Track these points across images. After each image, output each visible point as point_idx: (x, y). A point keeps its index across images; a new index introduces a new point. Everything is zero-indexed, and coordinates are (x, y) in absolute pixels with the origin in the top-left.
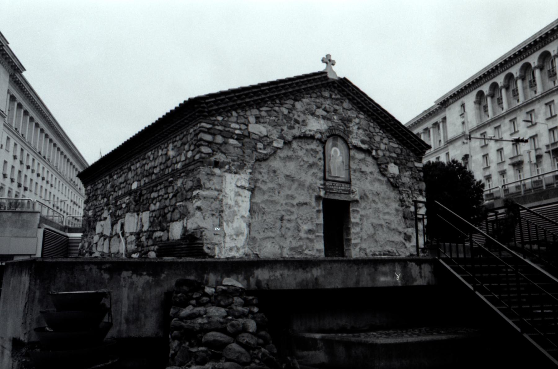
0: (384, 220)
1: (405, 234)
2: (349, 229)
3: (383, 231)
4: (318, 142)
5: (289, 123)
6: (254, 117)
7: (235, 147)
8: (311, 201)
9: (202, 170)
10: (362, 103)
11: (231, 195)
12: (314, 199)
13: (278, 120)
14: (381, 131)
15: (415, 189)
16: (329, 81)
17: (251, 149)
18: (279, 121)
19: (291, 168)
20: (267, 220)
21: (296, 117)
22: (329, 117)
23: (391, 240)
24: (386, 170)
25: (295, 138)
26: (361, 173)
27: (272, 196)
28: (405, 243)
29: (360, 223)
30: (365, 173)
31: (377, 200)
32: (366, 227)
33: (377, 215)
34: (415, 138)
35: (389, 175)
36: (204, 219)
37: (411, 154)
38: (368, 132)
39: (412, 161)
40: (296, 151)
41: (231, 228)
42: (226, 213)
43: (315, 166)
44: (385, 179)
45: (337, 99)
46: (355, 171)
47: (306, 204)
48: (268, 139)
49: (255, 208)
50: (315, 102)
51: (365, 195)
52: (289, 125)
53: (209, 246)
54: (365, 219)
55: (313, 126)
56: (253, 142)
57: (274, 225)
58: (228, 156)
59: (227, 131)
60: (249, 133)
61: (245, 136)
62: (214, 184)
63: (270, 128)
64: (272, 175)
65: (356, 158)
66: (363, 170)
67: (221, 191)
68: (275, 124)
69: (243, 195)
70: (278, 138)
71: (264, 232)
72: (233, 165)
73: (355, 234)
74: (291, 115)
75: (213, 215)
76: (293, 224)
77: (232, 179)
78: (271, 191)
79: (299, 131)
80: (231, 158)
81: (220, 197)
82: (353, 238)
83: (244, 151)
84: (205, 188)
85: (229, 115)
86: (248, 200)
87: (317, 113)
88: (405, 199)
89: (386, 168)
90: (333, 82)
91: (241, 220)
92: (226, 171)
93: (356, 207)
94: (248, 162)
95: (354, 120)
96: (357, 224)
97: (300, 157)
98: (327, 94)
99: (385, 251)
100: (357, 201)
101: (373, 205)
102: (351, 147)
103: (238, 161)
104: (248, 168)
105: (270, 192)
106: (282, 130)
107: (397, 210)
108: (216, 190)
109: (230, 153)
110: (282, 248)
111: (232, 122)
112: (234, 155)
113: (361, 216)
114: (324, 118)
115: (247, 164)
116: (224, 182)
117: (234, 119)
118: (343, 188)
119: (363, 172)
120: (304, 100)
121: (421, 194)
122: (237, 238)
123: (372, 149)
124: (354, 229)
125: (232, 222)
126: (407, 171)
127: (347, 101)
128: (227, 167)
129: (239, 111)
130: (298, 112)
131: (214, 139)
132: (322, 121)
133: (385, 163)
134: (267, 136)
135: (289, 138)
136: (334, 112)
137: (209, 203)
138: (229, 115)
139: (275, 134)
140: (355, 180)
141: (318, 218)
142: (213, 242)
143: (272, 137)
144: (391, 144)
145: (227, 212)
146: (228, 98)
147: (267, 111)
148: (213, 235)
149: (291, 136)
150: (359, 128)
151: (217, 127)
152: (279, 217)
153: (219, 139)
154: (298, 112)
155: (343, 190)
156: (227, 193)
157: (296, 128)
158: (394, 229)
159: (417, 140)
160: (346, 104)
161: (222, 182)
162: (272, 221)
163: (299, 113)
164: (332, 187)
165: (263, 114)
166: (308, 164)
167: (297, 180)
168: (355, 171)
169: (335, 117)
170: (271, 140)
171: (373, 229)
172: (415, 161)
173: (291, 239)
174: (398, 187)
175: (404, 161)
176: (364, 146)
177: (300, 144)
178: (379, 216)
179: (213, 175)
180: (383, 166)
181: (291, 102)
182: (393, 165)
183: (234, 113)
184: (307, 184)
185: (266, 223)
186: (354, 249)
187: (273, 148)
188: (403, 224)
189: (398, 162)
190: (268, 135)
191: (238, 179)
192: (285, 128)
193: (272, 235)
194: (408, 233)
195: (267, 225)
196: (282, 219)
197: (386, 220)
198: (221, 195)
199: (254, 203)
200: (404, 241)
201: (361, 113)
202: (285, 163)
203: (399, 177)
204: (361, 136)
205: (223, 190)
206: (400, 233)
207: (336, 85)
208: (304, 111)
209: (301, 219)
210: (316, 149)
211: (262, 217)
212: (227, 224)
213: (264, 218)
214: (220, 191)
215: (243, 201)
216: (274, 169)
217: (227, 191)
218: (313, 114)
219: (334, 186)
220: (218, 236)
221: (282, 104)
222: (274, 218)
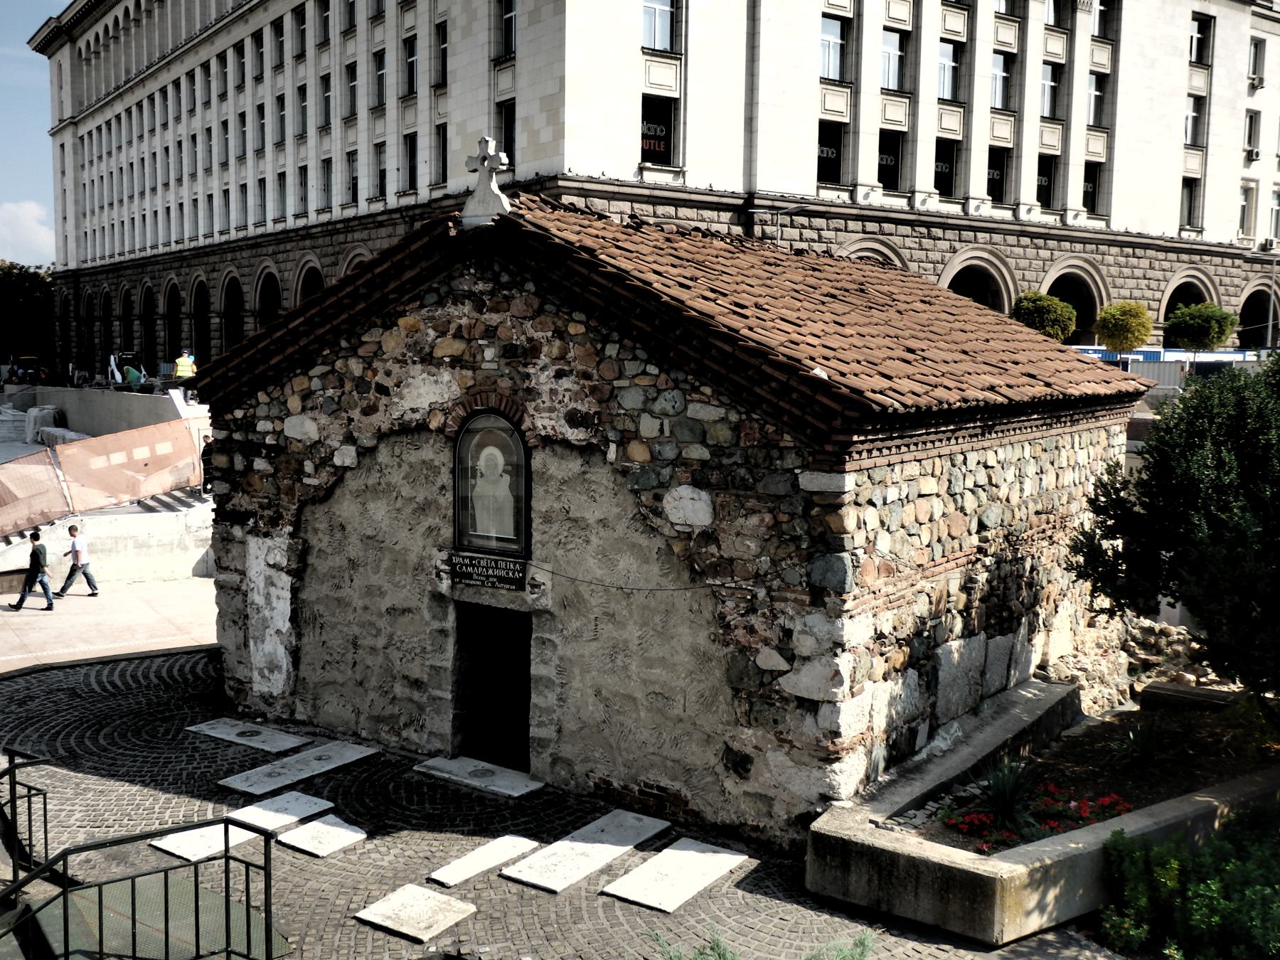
0: (645, 682)
5: (365, 398)
7: (263, 475)
11: (261, 583)
12: (426, 600)
13: (343, 393)
14: (652, 369)
15: (787, 586)
19: (379, 510)
20: (330, 644)
21: (379, 378)
24: (659, 513)
25: (381, 436)
26: (569, 524)
27: (339, 587)
29: (558, 682)
32: (579, 695)
33: (619, 662)
34: (783, 378)
37: (787, 440)
40: (386, 472)
42: (253, 622)
43: (433, 508)
44: (659, 542)
46: (547, 519)
47: (409, 610)
50: (432, 318)
51: (577, 594)
52: (365, 403)
53: (232, 683)
54: (577, 671)
55: (419, 395)
60: (287, 438)
63: (324, 419)
64: (338, 535)
65: (551, 477)
66: (571, 515)
68: (335, 407)
69: (280, 584)
70: (342, 443)
71: (323, 668)
72: (262, 517)
75: (234, 622)
86: (288, 595)
88: (733, 619)
91: (276, 638)
92: (249, 532)
95: (545, 349)
101: (607, 629)
102: (532, 442)
103: (269, 506)
106: (350, 420)
107: (703, 658)
108: (236, 570)
113: (561, 659)
114: (456, 362)
118: (503, 573)
119: (575, 520)
123: (607, 442)
124: (540, 693)
125: (263, 642)
128: (251, 522)
130: (385, 361)
131: (232, 462)
132: (446, 376)
133: (653, 488)
134: (319, 441)
135: (367, 442)
137: (229, 598)
138: (253, 402)
141: (441, 650)
143: (328, 442)
145: (253, 620)
146: (232, 369)
150: (559, 375)
155: (501, 579)
156: (253, 579)
157: (382, 408)
163: (389, 365)
164: (470, 569)
165: (316, 384)
167: (389, 549)
168: (547, 519)
169: (489, 353)
171: (601, 706)
172: (805, 467)
175: (742, 471)
176: (575, 435)
178: (625, 668)
182: (685, 491)
183: (262, 397)
184: (413, 558)
188: (723, 707)
189: (714, 477)
191: (269, 549)
192: (356, 414)
193: (340, 679)
194: (736, 746)
196: (355, 645)
197: (653, 683)
200: (720, 769)
203: (709, 536)
204: (566, 400)
208: (404, 355)
209: (398, 648)
210: (432, 460)
212: (255, 644)
213: (324, 638)
214: (243, 573)
215: (278, 598)
217: (252, 573)
218: (429, 360)
219: (473, 566)
221: (353, 351)
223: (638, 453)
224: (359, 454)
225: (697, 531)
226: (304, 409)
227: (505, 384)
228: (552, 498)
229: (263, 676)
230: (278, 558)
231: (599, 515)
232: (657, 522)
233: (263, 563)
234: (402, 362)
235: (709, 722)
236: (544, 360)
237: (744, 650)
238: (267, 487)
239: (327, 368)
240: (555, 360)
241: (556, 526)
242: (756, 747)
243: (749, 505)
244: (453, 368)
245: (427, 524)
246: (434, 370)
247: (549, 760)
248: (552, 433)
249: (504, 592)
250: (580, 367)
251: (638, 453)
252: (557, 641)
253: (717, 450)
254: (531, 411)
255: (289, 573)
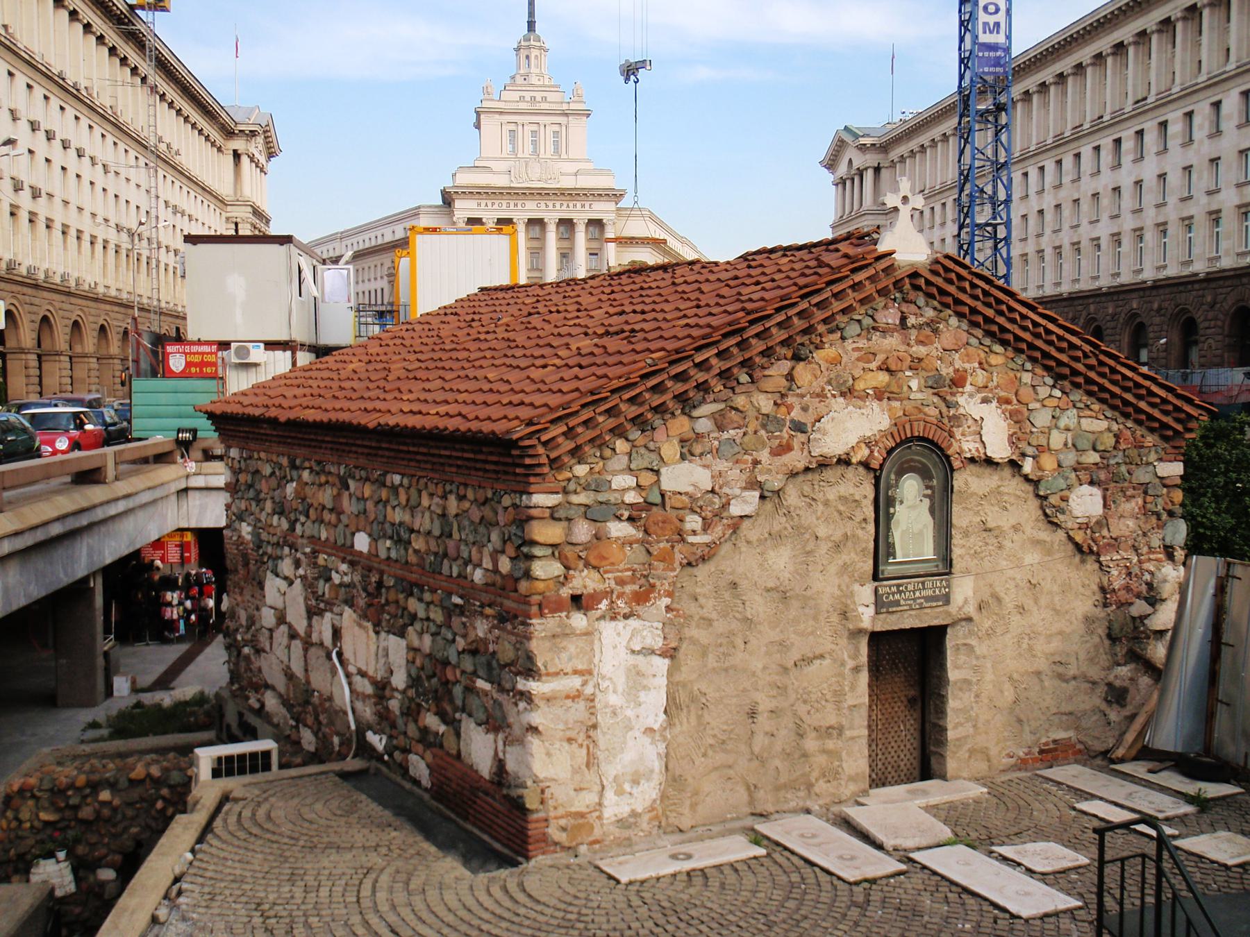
1: (1109, 685)
2: (942, 699)
3: (1043, 688)
4: (861, 469)
6: (676, 442)
8: (834, 647)
9: (537, 627)
10: (1001, 320)
12: (844, 642)
14: (1057, 393)
16: (899, 274)
17: (668, 541)
18: (746, 439)
19: (781, 560)
21: (796, 414)
22: (895, 389)
23: (1063, 710)
25: (793, 475)
26: (985, 534)
28: (1108, 711)
30: (996, 533)
31: (1028, 604)
32: (991, 687)
35: (1069, 525)
36: (548, 754)
37: (1150, 440)
38: (1015, 406)
39: (1148, 464)
41: (619, 767)
43: (849, 544)
44: (1061, 534)
45: (920, 327)
48: (717, 500)
49: (682, 697)
53: (563, 822)
56: (672, 514)
57: (732, 731)
58: (606, 572)
59: (601, 503)
61: (649, 505)
62: (570, 659)
63: (722, 465)
64: (727, 595)
65: (974, 494)
66: (991, 524)
67: (590, 672)
68: (737, 449)
70: (745, 489)
71: (704, 755)
72: (620, 596)
73: (956, 711)
74: (783, 409)
75: (570, 740)
76: (788, 721)
77: (619, 634)
78: (724, 641)
79: (805, 452)
80: (615, 578)
81: (589, 690)
82: (950, 726)
83: (651, 549)
84: (548, 674)
85: (608, 453)
86: (664, 681)
87: (860, 386)
89: (1063, 505)
90: (915, 275)
91: (646, 740)
92: (602, 617)
93: (965, 637)
94: (659, 578)
95: (969, 379)
96: (967, 682)
97: (807, 529)
98: (890, 316)
99: (1046, 744)
100: (969, 619)
101: (1016, 618)
103: (633, 580)
104: (660, 596)
105: (721, 645)
106: (756, 462)
108: (576, 672)
109: (613, 564)
110: (751, 789)
111: (615, 473)
112: (622, 566)
114: (879, 395)
115: (658, 583)
116: (597, 647)
117: (620, 462)
118: (930, 593)
120: (818, 355)
121: (1170, 556)
122: (635, 791)
123: (1024, 455)
126: (1129, 498)
127: (954, 321)
128: (604, 605)
129: (635, 434)
130: (803, 396)
134: (713, 491)
136: (911, 368)
137: (560, 711)
138: (608, 453)
139: (735, 475)
140: (967, 557)
141: (853, 687)
142: (573, 810)
143: (726, 490)
144: (1087, 424)
147: (712, 416)
148: (572, 793)
149: (780, 476)
151: (575, 499)
152: (747, 709)
153: (583, 532)
154: (803, 396)
155: (928, 599)
157: (796, 444)
158: (1075, 678)
159: (1171, 398)
160: (953, 328)
161: (592, 649)
162: (726, 723)
164: (897, 597)
166: (830, 544)
168: (966, 534)
169: (914, 384)
170: (724, 500)
171: (1012, 690)
172: (1160, 460)
173: (777, 762)
174: (1098, 555)
175: (1123, 469)
177: (807, 489)
178: (1031, 648)
179: (566, 633)
180: (1054, 500)
181: (785, 366)
182: (1086, 489)
183: (621, 445)
184: (826, 603)
185: (711, 732)
186: (955, 753)
187: (730, 522)
189: (1102, 475)
190: (717, 488)
192: (764, 456)
194: (1118, 683)
195: (714, 736)
198: (591, 684)
199: (678, 683)
200: (1104, 706)
201: (998, 348)
202: (761, 554)
203: (1103, 522)
205: (595, 673)
206: (1094, 683)
207: (922, 282)
208: (823, 390)
209: (805, 702)
211: (699, 717)
216: (731, 577)
218: (848, 393)
219: (900, 592)
220: (584, 792)
222: (730, 712)
223: (1048, 462)
224: (762, 497)
225: (1094, 520)
226: (683, 457)
227: (933, 412)
228: (971, 513)
229: (620, 792)
230: (649, 642)
231: (1013, 521)
232: (1061, 517)
233: (623, 654)
234: (821, 396)
235: (1095, 673)
236: (968, 388)
237: (1121, 605)
238: (635, 555)
239: (722, 406)
240: (980, 389)
241: (972, 539)
242: (1131, 679)
243: (1128, 493)
244: (880, 399)
245: (841, 562)
246: (860, 403)
247: (967, 755)
248: (976, 454)
249: (928, 611)
250: (1002, 394)
251: (1048, 462)
252: (973, 642)
253: (1104, 453)
254: (958, 436)
255: (663, 655)
